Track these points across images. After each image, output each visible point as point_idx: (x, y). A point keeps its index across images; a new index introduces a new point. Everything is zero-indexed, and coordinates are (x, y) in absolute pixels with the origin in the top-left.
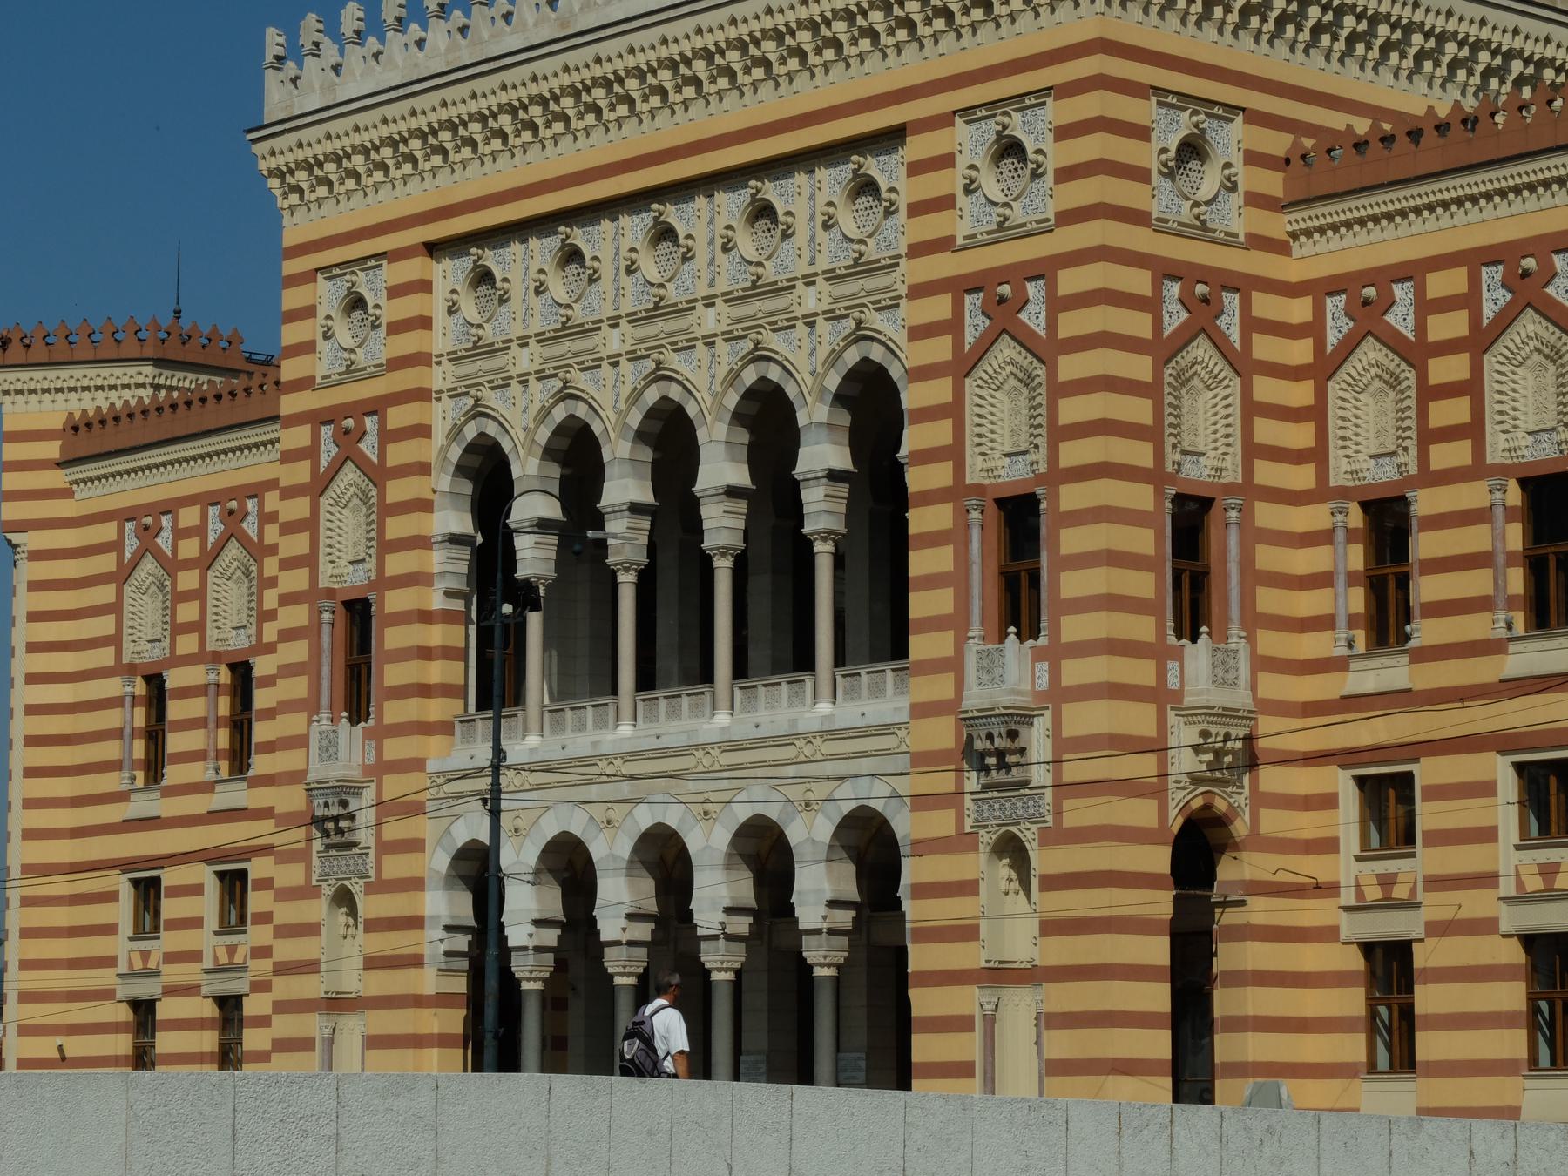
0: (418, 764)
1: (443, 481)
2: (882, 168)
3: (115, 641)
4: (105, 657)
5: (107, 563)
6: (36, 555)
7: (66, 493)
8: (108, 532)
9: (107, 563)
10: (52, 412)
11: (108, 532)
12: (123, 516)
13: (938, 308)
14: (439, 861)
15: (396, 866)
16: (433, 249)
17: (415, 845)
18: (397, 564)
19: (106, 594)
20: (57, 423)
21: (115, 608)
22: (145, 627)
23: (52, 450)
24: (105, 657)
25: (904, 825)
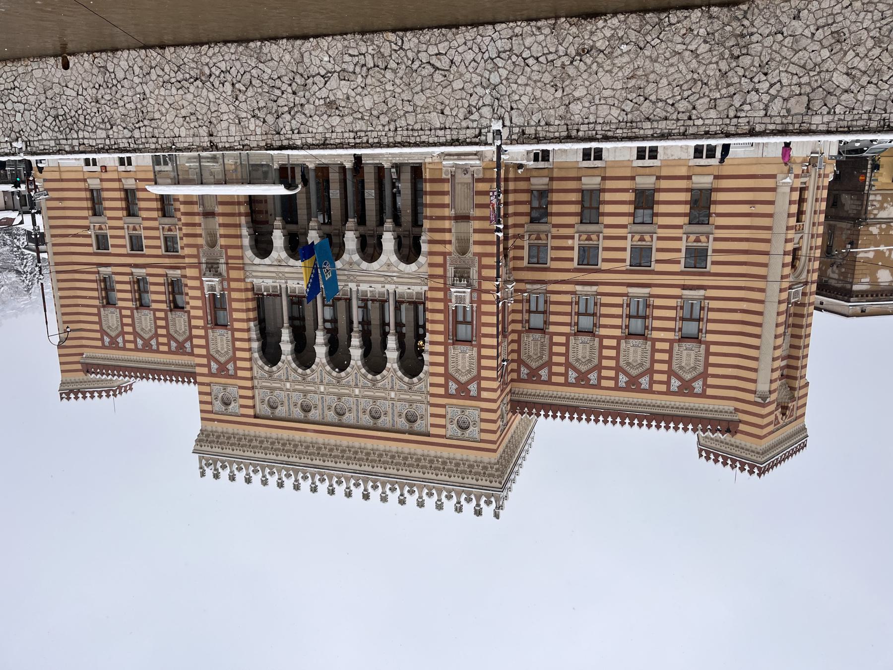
0: (431, 289)
1: (425, 368)
2: (264, 409)
3: (708, 353)
4: (713, 349)
5: (710, 381)
6: (754, 392)
7: (736, 410)
8: (710, 392)
9: (710, 381)
10: (739, 439)
11: (710, 392)
12: (703, 395)
13: (240, 373)
14: (422, 259)
15: (439, 260)
16: (428, 435)
17: (431, 265)
18: (441, 349)
19: (711, 370)
20: (738, 435)
21: (707, 365)
22: (688, 357)
23: (742, 427)
24: (713, 349)
25: (249, 253)
